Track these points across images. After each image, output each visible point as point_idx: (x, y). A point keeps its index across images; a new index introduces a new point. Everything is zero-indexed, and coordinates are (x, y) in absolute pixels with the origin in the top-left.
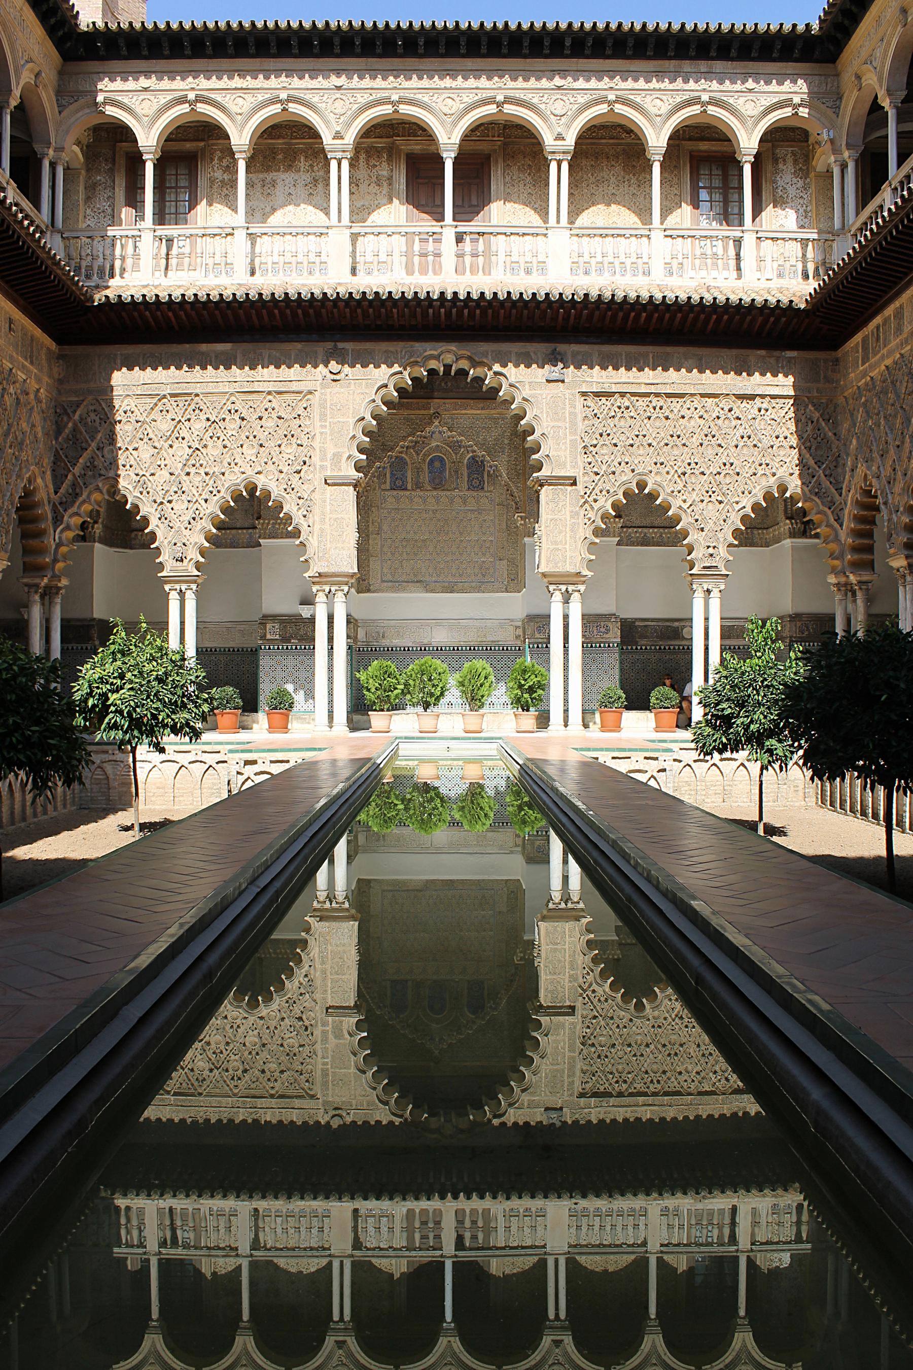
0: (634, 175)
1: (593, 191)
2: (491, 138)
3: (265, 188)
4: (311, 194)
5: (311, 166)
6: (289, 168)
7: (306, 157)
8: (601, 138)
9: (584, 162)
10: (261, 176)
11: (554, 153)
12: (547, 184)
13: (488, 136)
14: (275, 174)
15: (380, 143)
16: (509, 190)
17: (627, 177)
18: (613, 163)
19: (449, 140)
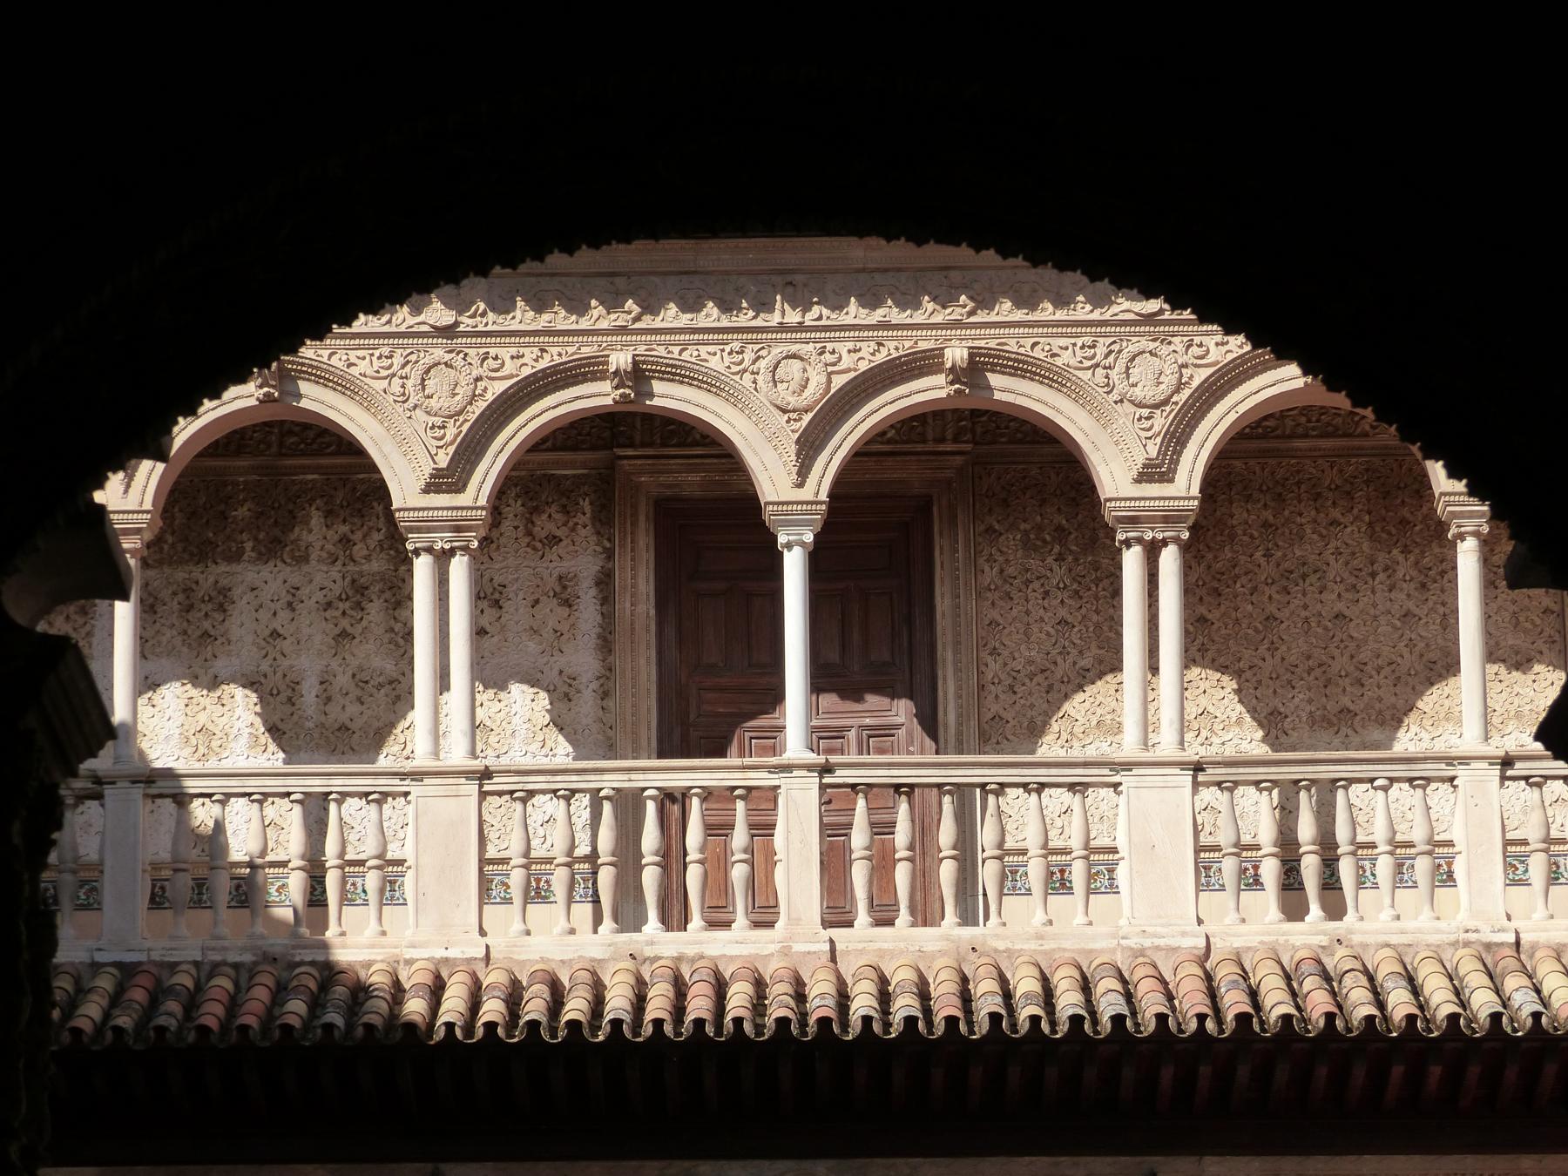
0: (1406, 551)
1: (1272, 609)
2: (930, 447)
3: (193, 616)
4: (344, 634)
5: (345, 541)
6: (273, 548)
7: (329, 514)
8: (1292, 436)
9: (1239, 514)
10: (180, 575)
11: (1133, 521)
12: (1117, 592)
13: (924, 441)
14: (223, 568)
15: (572, 465)
16: (994, 614)
17: (1382, 558)
18: (1336, 514)
19: (790, 487)
